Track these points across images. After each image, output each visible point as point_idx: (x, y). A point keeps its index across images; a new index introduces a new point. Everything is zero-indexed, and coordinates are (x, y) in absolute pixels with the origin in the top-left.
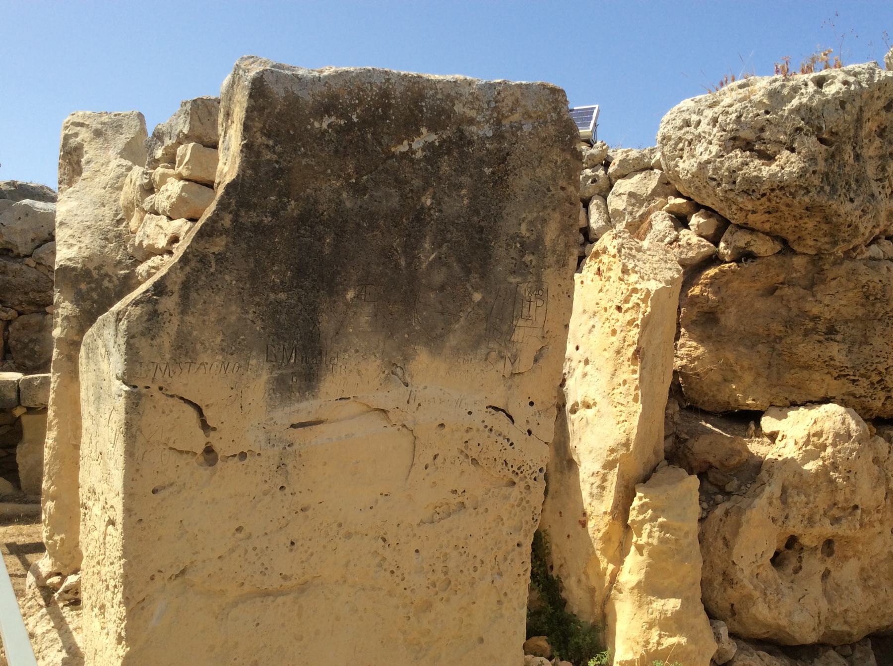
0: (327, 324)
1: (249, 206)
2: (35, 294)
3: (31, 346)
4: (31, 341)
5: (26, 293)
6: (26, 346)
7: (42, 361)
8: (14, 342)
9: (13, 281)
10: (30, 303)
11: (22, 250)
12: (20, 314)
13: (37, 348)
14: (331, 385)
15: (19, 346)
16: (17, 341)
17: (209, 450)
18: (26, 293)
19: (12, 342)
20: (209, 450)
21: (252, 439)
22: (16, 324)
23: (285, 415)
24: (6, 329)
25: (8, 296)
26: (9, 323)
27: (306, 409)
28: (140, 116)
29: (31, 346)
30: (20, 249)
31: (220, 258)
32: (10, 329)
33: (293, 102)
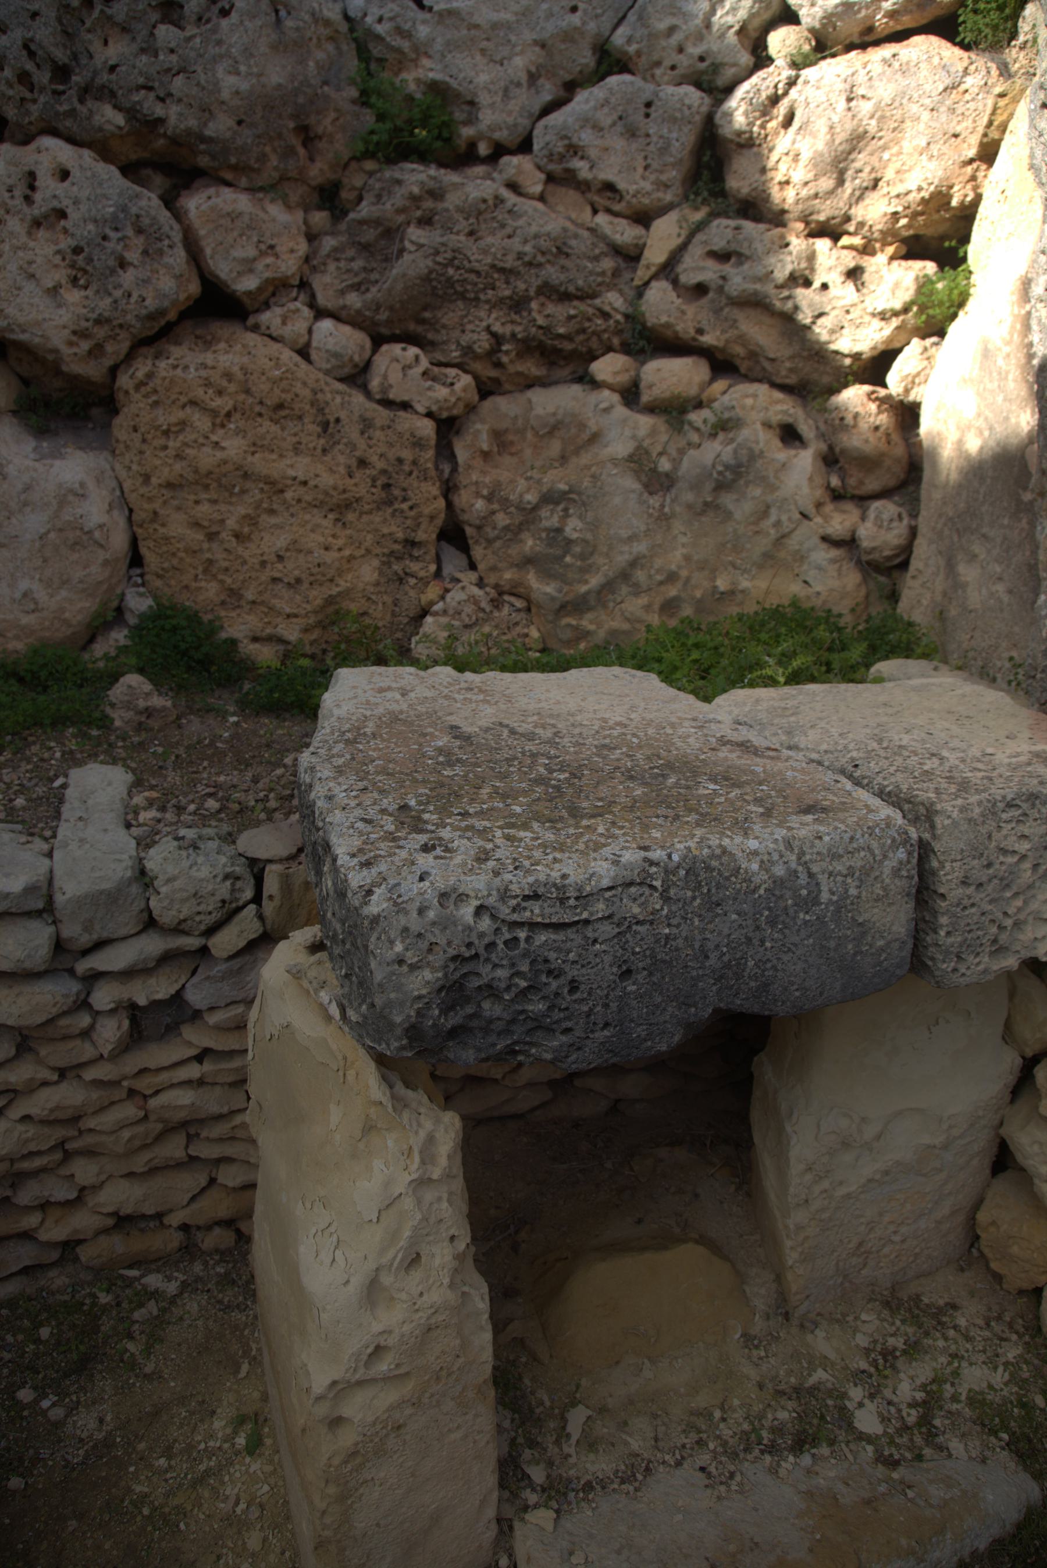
2: (551, 308)
3: (549, 518)
4: (550, 498)
5: (518, 304)
6: (529, 515)
7: (595, 581)
8: (480, 504)
9: (472, 250)
10: (529, 347)
12: (486, 390)
13: (573, 527)
15: (502, 519)
16: (489, 499)
18: (518, 304)
22: (478, 434)
24: (445, 449)
25: (450, 316)
26: (448, 426)
29: (549, 518)
30: (487, 118)
32: (462, 454)
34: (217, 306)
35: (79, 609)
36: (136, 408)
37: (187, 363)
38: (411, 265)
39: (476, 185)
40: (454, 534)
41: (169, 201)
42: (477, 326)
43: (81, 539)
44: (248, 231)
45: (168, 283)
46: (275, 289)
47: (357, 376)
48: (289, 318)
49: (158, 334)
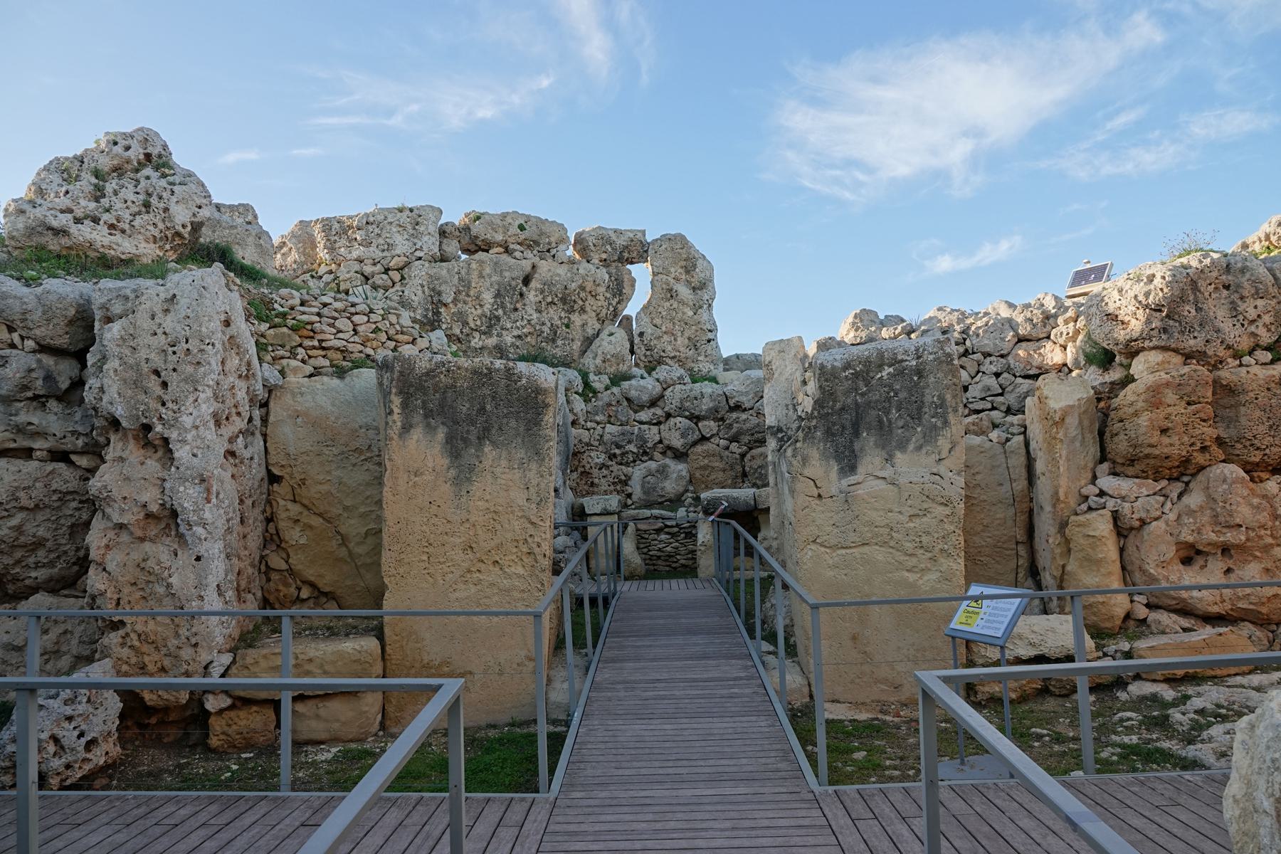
0: (857, 446)
1: (823, 408)
11: (747, 405)
12: (751, 449)
14: (861, 470)
17: (820, 496)
19: (747, 469)
20: (820, 496)
21: (834, 491)
22: (748, 456)
23: (845, 482)
26: (743, 456)
27: (853, 479)
28: (800, 338)
31: (815, 427)
33: (833, 367)
34: (704, 439)
35: (681, 489)
36: (692, 457)
37: (699, 448)
38: (734, 430)
39: (744, 416)
40: (745, 475)
41: (696, 424)
42: (746, 439)
43: (681, 477)
44: (709, 426)
45: (696, 436)
46: (712, 436)
47: (727, 448)
48: (715, 440)
49: (695, 444)
